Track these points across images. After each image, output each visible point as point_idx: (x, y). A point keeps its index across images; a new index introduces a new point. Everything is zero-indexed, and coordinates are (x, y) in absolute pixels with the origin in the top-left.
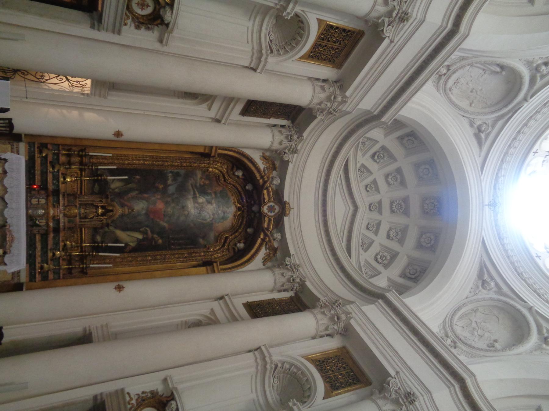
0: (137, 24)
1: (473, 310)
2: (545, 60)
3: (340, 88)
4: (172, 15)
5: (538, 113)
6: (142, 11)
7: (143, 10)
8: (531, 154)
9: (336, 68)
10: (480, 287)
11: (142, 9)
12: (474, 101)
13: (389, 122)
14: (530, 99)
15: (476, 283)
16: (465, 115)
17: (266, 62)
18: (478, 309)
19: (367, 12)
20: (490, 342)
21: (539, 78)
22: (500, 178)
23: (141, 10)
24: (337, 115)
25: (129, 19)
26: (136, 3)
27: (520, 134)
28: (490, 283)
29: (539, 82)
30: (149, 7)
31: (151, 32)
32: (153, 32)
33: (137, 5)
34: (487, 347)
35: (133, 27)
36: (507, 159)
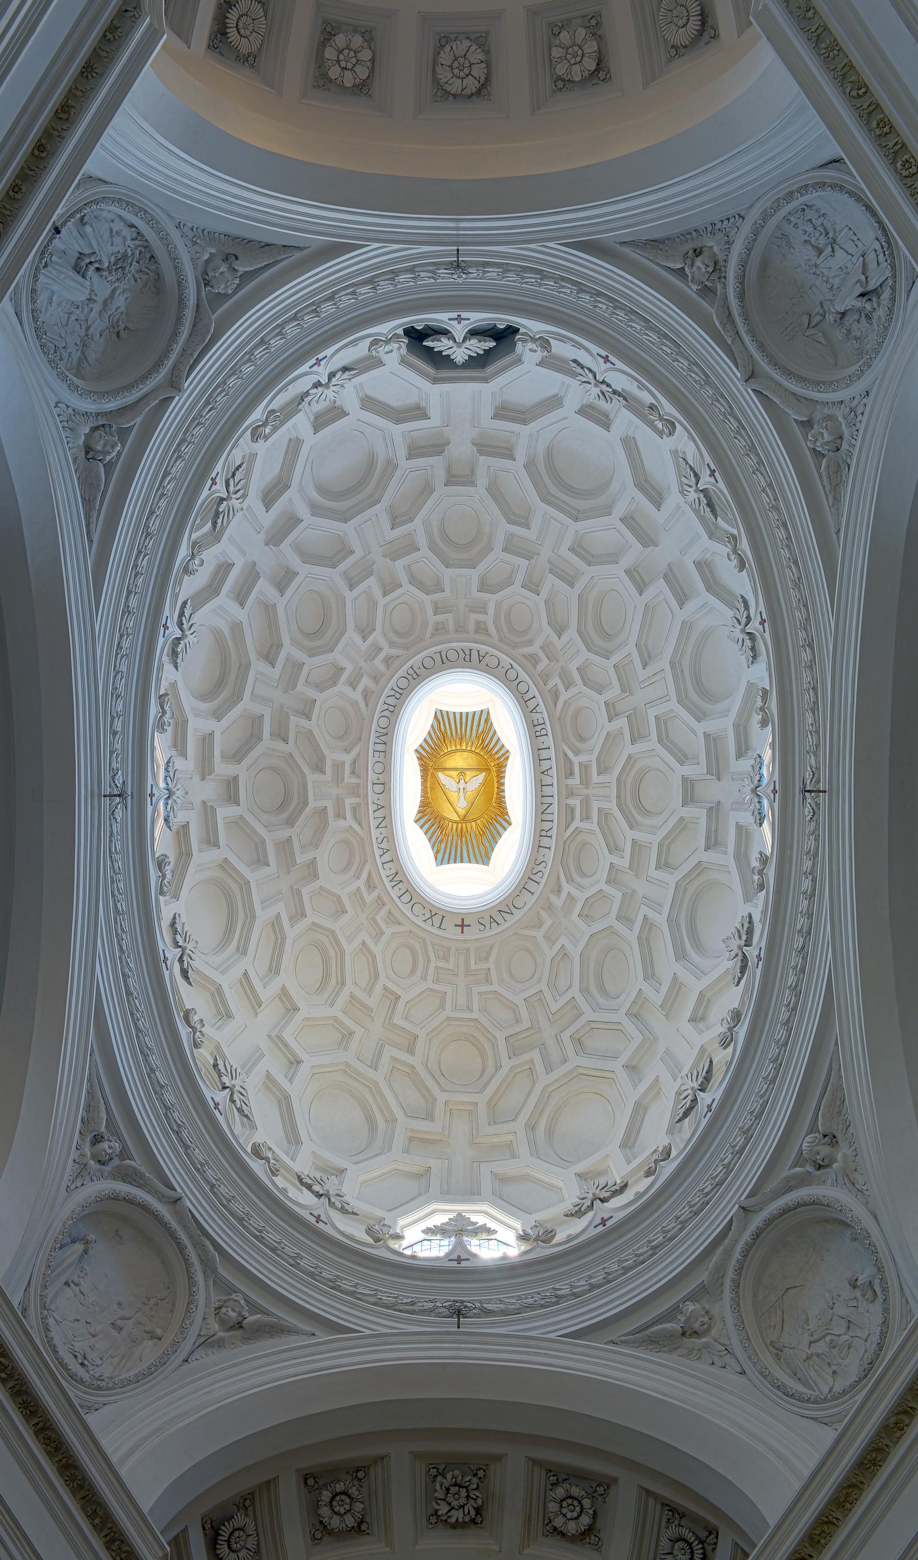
1: (777, 1355)
2: (88, 1140)
5: (215, 1190)
8: (321, 1225)
10: (704, 1340)
12: (147, 1329)
13: (162, 1547)
14: (176, 1190)
15: (695, 1352)
16: (184, 1356)
18: (771, 1342)
20: (860, 1298)
21: (128, 1162)
22: (381, 1299)
27: (263, 1238)
28: (688, 1314)
29: (137, 1163)
34: (876, 1302)
36: (330, 1277)
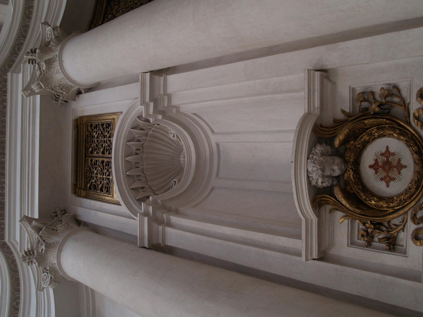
0: (396, 100)
3: (55, 96)
4: (308, 177)
6: (387, 147)
7: (384, 150)
9: (82, 118)
11: (387, 153)
17: (143, 102)
19: (62, 253)
23: (392, 150)
24: (25, 57)
25: (414, 116)
26: (405, 167)
30: (373, 162)
31: (359, 90)
32: (353, 90)
33: (403, 162)
35: (403, 85)
